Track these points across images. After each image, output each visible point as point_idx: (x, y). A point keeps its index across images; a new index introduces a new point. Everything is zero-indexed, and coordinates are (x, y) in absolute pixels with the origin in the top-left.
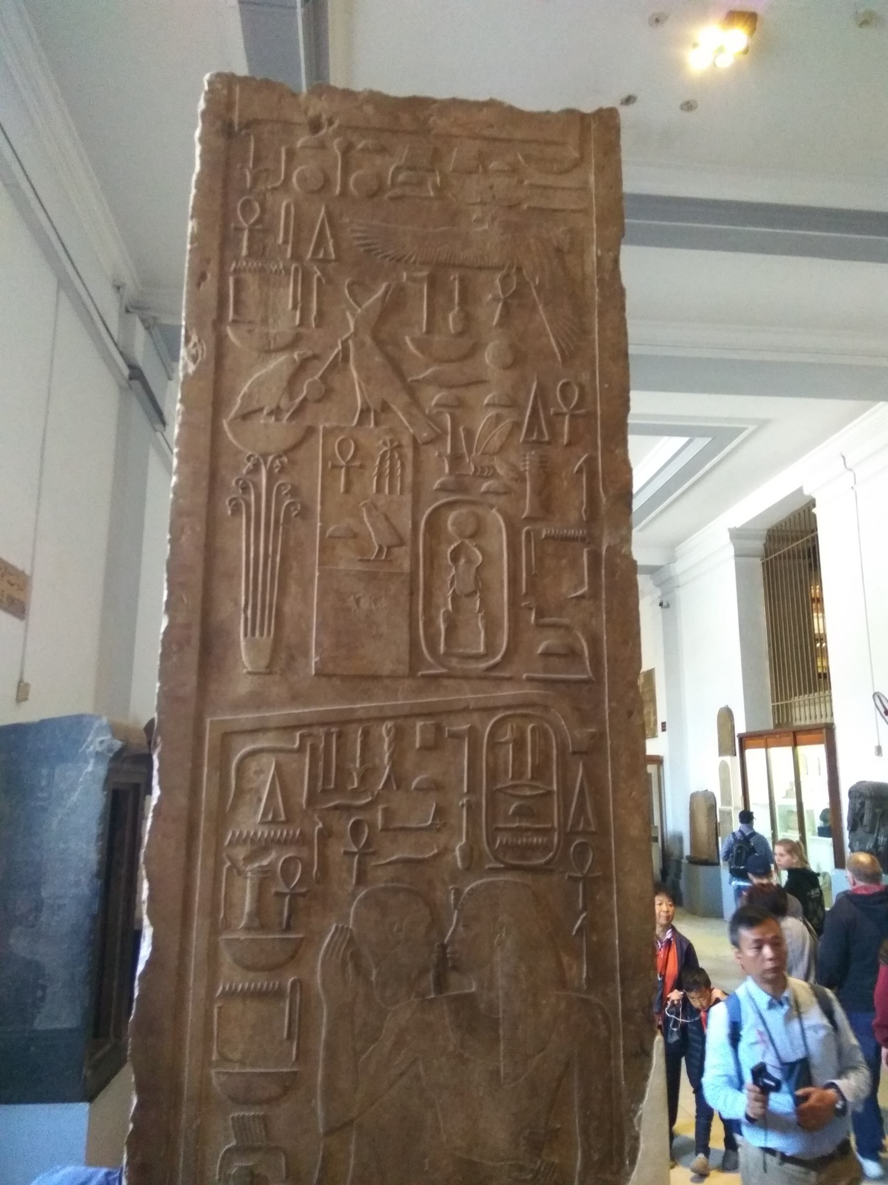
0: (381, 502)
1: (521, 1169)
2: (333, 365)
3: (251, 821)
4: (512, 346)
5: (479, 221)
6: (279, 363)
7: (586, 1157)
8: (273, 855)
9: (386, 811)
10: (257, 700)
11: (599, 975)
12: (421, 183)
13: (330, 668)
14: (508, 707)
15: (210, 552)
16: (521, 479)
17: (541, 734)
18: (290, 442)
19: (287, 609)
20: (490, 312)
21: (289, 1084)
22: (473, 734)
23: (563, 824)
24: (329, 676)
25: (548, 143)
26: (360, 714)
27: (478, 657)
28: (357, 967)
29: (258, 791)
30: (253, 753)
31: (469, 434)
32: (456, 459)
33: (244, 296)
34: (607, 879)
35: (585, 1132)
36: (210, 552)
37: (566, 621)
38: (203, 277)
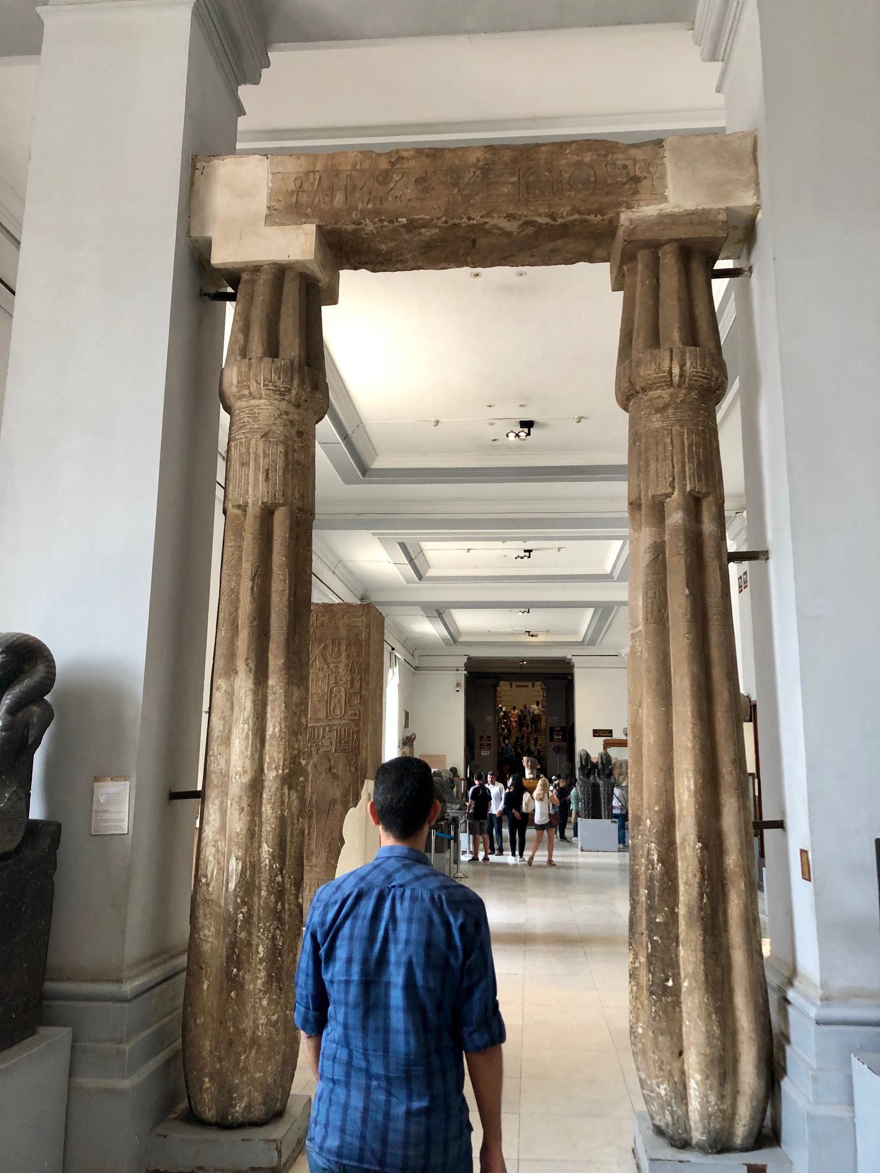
20: (343, 648)
32: (336, 678)
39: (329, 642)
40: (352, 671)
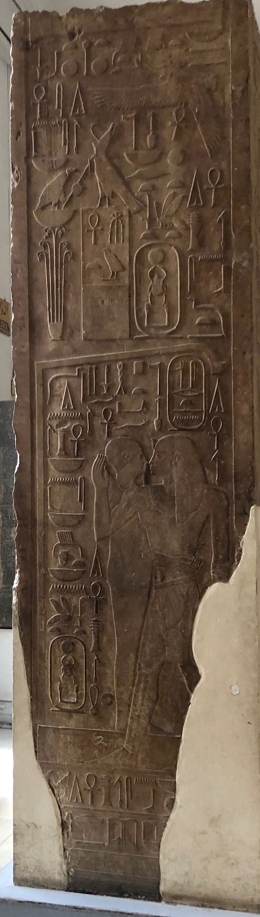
0: (113, 248)
1: (186, 560)
2: (86, 174)
3: (57, 409)
4: (183, 152)
5: (164, 78)
6: (58, 177)
7: (216, 557)
8: (69, 424)
9: (120, 404)
10: (57, 353)
11: (223, 478)
12: (130, 60)
13: (90, 336)
14: (179, 352)
15: (31, 281)
16: (187, 228)
17: (196, 364)
18: (66, 219)
19: (69, 308)
20: (169, 132)
21: (81, 520)
22: (162, 366)
23: (207, 411)
24: (90, 340)
25: (203, 22)
26: (106, 359)
27: (165, 328)
28: (109, 473)
29: (60, 396)
30: (57, 378)
31: (159, 205)
32: (151, 221)
33: (40, 141)
34: (230, 435)
35: (216, 546)
36: (31, 281)
37: (211, 306)
38: (19, 134)
39: (127, 120)
40: (197, 197)
